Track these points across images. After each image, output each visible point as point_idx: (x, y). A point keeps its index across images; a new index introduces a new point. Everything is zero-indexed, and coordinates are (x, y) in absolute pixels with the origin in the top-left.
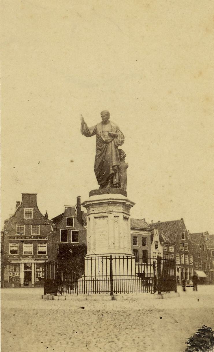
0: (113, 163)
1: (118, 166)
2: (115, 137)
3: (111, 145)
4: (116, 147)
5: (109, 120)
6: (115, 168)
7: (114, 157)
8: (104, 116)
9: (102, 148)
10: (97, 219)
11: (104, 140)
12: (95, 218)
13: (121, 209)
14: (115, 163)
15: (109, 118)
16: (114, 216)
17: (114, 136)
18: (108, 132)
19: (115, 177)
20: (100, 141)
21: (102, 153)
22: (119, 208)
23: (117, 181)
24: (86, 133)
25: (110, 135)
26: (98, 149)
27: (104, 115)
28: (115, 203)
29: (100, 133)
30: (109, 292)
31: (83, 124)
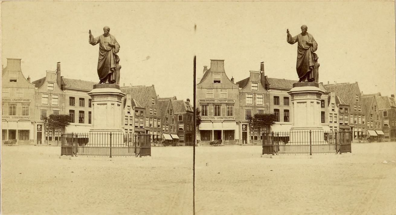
10: (99, 106)
13: (116, 99)
19: (112, 76)
28: (111, 95)
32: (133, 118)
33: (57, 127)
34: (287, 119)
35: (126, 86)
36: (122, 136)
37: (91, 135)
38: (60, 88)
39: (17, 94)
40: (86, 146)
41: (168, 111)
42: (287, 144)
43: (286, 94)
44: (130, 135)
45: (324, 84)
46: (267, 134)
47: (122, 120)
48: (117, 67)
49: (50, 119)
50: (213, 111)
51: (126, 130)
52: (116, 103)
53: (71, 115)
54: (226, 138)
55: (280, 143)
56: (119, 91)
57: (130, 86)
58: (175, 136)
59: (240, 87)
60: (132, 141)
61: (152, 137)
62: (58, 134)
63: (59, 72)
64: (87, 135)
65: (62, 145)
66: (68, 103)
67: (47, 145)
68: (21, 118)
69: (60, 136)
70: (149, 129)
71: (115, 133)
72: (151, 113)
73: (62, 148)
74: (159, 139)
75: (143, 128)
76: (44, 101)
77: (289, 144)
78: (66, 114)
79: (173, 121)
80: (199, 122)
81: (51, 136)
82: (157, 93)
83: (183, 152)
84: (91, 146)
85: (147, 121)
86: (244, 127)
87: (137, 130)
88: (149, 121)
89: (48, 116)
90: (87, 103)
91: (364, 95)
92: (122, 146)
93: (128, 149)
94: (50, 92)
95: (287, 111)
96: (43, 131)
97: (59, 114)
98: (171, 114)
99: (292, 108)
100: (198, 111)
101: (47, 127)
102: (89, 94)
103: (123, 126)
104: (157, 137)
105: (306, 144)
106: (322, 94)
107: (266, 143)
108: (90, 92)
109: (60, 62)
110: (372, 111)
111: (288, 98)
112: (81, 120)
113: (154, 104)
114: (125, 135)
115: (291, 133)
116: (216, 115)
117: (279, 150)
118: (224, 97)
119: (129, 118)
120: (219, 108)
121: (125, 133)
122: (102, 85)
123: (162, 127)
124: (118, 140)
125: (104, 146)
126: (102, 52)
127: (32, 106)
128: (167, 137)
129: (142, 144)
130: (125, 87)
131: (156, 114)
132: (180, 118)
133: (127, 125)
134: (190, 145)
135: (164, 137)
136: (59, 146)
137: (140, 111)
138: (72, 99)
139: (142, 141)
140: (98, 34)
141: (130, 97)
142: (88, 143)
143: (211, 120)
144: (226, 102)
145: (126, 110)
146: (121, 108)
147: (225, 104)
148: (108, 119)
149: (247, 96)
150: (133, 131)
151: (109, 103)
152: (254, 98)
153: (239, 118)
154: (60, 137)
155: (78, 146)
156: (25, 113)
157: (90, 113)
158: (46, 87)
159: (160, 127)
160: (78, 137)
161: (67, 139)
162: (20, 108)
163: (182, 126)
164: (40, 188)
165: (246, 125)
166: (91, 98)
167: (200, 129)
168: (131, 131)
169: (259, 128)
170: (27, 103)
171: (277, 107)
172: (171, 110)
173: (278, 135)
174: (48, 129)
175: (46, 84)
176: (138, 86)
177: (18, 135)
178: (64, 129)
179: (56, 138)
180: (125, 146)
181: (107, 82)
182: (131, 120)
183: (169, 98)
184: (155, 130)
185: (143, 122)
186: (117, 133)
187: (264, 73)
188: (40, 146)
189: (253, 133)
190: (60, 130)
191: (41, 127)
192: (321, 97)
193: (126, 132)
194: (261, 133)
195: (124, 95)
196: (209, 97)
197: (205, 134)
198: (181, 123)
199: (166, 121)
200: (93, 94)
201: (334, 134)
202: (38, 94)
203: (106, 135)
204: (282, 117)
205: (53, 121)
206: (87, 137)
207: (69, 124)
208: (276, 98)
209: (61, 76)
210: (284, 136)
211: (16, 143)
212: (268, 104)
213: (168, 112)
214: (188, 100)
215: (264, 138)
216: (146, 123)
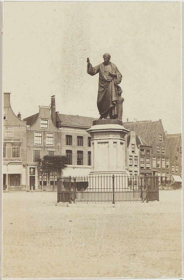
0: (113, 98)
1: (116, 101)
2: (115, 77)
3: (111, 84)
4: (115, 85)
5: (110, 61)
6: (114, 102)
7: (114, 94)
8: (106, 59)
9: (104, 86)
10: (100, 144)
11: (106, 79)
12: (98, 143)
13: (118, 137)
14: (114, 99)
15: (110, 60)
16: (114, 142)
17: (114, 77)
18: (109, 72)
20: (102, 80)
21: (104, 90)
22: (117, 136)
23: (116, 114)
24: (91, 71)
25: (110, 75)
26: (100, 86)
27: (106, 58)
29: (103, 73)
30: (111, 201)
31: (89, 65)
33: (52, 170)
35: (129, 121)
36: (127, 178)
37: (91, 178)
38: (56, 124)
39: (7, 133)
40: (86, 191)
41: (178, 149)
47: (126, 161)
48: (119, 99)
49: (45, 160)
51: (130, 171)
53: (68, 155)
56: (122, 127)
57: (134, 121)
60: (138, 185)
61: (160, 179)
62: (54, 178)
63: (54, 107)
64: (86, 178)
65: (58, 191)
66: (65, 143)
67: (41, 191)
68: (11, 160)
69: (56, 180)
70: (156, 170)
71: (118, 175)
72: (158, 152)
73: (58, 194)
74: (168, 181)
75: (150, 169)
76: (37, 141)
81: (45, 180)
84: (92, 190)
85: (154, 161)
89: (42, 157)
90: (86, 141)
92: (127, 190)
93: (133, 193)
94: (43, 130)
96: (36, 175)
97: (55, 155)
101: (41, 170)
102: (88, 131)
103: (127, 167)
104: (166, 179)
108: (89, 129)
109: (54, 96)
112: (80, 162)
113: (161, 141)
114: (130, 178)
119: (134, 158)
121: (129, 175)
122: (103, 120)
123: (171, 168)
124: (122, 184)
126: (102, 84)
127: (24, 147)
129: (149, 187)
130: (128, 123)
131: (164, 153)
133: (132, 166)
135: (173, 179)
136: (55, 192)
138: (69, 138)
140: (97, 62)
141: (135, 134)
142: (88, 188)
145: (130, 150)
146: (124, 147)
148: (109, 159)
150: (138, 173)
151: (111, 142)
154: (56, 181)
155: (77, 191)
157: (89, 153)
160: (77, 181)
161: (64, 183)
162: (10, 149)
164: (34, 239)
166: (90, 136)
168: (136, 173)
174: (42, 172)
176: (143, 121)
177: (8, 180)
178: (60, 172)
179: (52, 183)
180: (129, 190)
181: (108, 117)
182: (135, 160)
183: (178, 134)
184: (163, 170)
185: (149, 162)
186: (121, 175)
188: (33, 191)
190: (56, 173)
191: (34, 171)
193: (130, 174)
195: (128, 131)
199: (175, 161)
200: (93, 131)
202: (30, 133)
203: (108, 178)
205: (47, 163)
206: (86, 181)
207: (66, 166)
209: (56, 111)
211: (6, 189)
213: (178, 150)
216: (154, 164)
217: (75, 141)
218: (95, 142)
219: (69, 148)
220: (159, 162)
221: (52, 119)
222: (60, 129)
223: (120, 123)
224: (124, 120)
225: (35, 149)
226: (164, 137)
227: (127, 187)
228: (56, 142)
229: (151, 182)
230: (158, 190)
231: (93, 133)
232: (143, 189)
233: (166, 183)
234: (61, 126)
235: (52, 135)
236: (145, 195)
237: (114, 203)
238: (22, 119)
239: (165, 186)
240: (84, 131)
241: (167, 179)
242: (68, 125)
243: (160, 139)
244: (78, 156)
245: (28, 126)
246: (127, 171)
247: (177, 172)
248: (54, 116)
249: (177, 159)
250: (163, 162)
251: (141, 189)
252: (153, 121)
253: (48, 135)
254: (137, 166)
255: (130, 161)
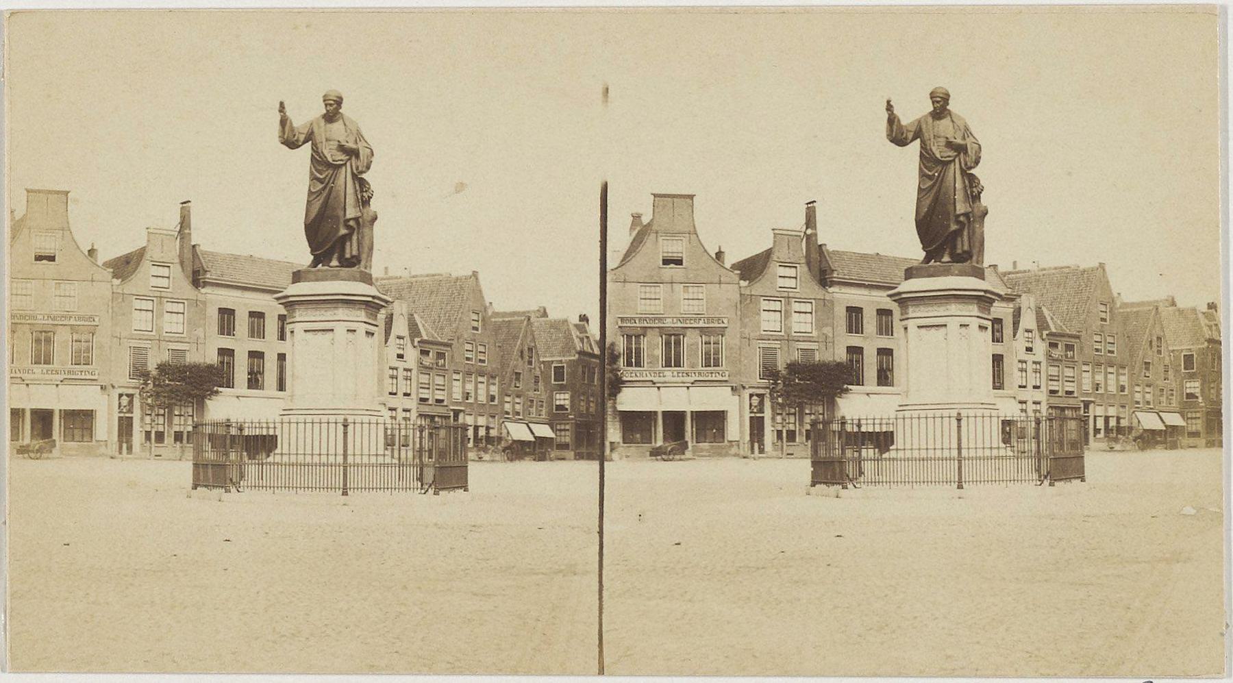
10: (309, 335)
13: (362, 315)
32: (414, 372)
34: (886, 377)
36: (381, 427)
42: (886, 455)
43: (882, 299)
44: (403, 426)
45: (1001, 269)
46: (827, 423)
47: (380, 381)
50: (659, 352)
51: (390, 409)
52: (362, 328)
53: (222, 363)
54: (700, 436)
55: (864, 452)
56: (372, 291)
57: (405, 274)
58: (544, 431)
59: (743, 277)
61: (470, 433)
71: (358, 419)
72: (468, 359)
76: (141, 321)
77: (893, 454)
78: (209, 362)
79: (537, 382)
80: (617, 385)
82: (488, 297)
83: (571, 477)
85: (455, 383)
86: (755, 400)
87: (426, 410)
88: (464, 382)
90: (271, 326)
91: (1125, 305)
92: (381, 460)
94: (158, 294)
95: (885, 353)
98: (530, 363)
99: (902, 342)
100: (613, 350)
102: (278, 299)
103: (382, 399)
104: (488, 433)
105: (946, 454)
106: (994, 300)
107: (822, 453)
110: (1150, 353)
111: (889, 313)
112: (255, 381)
115: (900, 422)
116: (668, 365)
117: (861, 473)
118: (695, 307)
120: (678, 343)
121: (389, 421)
123: (502, 403)
124: (368, 443)
125: (324, 459)
127: (102, 338)
128: (518, 432)
129: (442, 454)
131: (483, 361)
132: (559, 372)
134: (590, 457)
137: (435, 353)
139: (442, 444)
141: (405, 311)
143: (655, 380)
144: (701, 324)
145: (392, 349)
147: (698, 331)
148: (337, 377)
149: (764, 305)
151: (340, 329)
152: (786, 311)
153: (739, 373)
156: (82, 358)
157: (282, 357)
158: (147, 277)
159: (496, 402)
163: (563, 399)
165: (761, 396)
166: (284, 312)
167: (620, 408)
169: (801, 406)
170: (86, 329)
171: (855, 341)
172: (530, 350)
173: (859, 426)
175: (146, 266)
180: (388, 460)
184: (480, 409)
187: (816, 235)
189: (784, 419)
192: (992, 309)
194: (807, 419)
195: (387, 302)
196: (648, 308)
197: (637, 424)
198: (562, 388)
201: (1033, 424)
203: (332, 426)
204: (871, 372)
206: (271, 432)
208: (854, 313)
210: (877, 430)
212: (827, 330)
213: (522, 357)
214: (584, 318)
215: (817, 435)
216: (454, 389)
217: (242, 323)
218: (298, 328)
219: (226, 342)
220: (470, 387)
221: (182, 263)
222: (203, 291)
223: (367, 279)
224: (376, 271)
225: (134, 343)
226: (483, 320)
227: (381, 452)
228: (192, 324)
229: (447, 437)
230: (466, 460)
231: (290, 304)
232: (426, 459)
233: (487, 442)
234: (205, 284)
235: (180, 308)
236: (429, 474)
237: (345, 493)
238: (100, 263)
239: (485, 450)
240: (268, 297)
241: (491, 431)
242: (227, 279)
243: (475, 324)
244: (251, 366)
245: (117, 282)
246: (382, 408)
247: (518, 414)
248: (188, 255)
249: (518, 379)
250: (480, 386)
251: (421, 457)
252: (454, 275)
253: (169, 307)
254: (408, 395)
255: (390, 381)
